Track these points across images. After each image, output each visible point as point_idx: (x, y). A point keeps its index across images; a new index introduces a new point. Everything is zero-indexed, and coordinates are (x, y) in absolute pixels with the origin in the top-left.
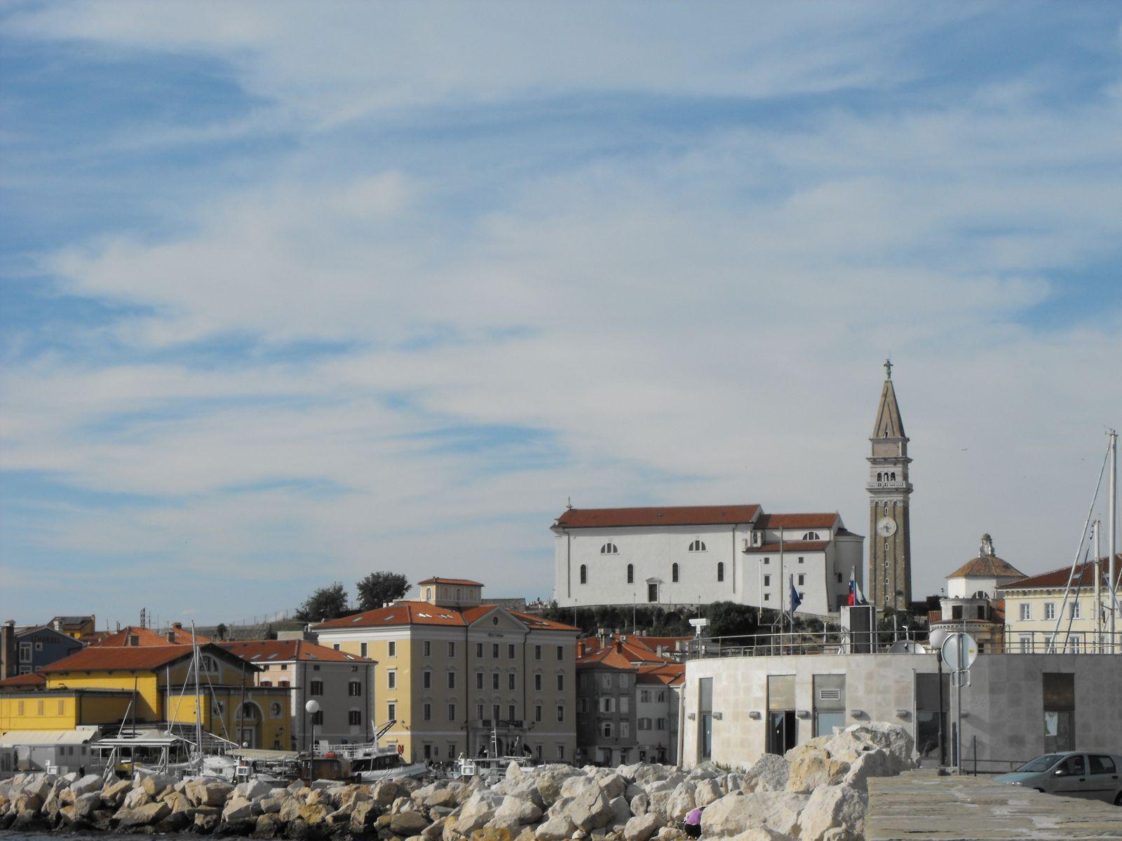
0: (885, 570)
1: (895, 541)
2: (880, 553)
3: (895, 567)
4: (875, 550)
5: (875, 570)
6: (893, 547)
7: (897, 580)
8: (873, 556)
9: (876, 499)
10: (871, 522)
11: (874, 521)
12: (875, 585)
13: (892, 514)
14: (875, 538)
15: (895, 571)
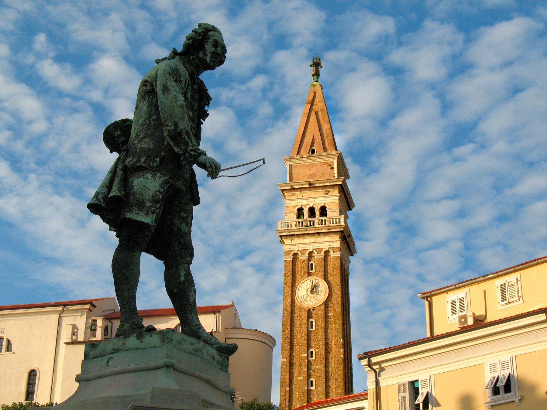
0: (309, 364)
1: (326, 316)
2: (300, 337)
3: (327, 358)
4: (292, 331)
5: (291, 365)
6: (323, 325)
7: (331, 382)
8: (288, 340)
9: (295, 249)
10: (286, 284)
11: (290, 284)
12: (291, 391)
13: (322, 270)
14: (292, 312)
15: (327, 366)
